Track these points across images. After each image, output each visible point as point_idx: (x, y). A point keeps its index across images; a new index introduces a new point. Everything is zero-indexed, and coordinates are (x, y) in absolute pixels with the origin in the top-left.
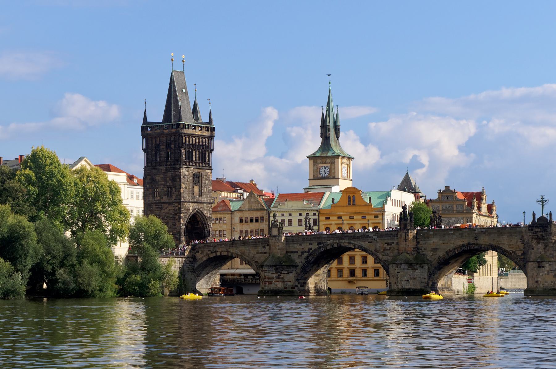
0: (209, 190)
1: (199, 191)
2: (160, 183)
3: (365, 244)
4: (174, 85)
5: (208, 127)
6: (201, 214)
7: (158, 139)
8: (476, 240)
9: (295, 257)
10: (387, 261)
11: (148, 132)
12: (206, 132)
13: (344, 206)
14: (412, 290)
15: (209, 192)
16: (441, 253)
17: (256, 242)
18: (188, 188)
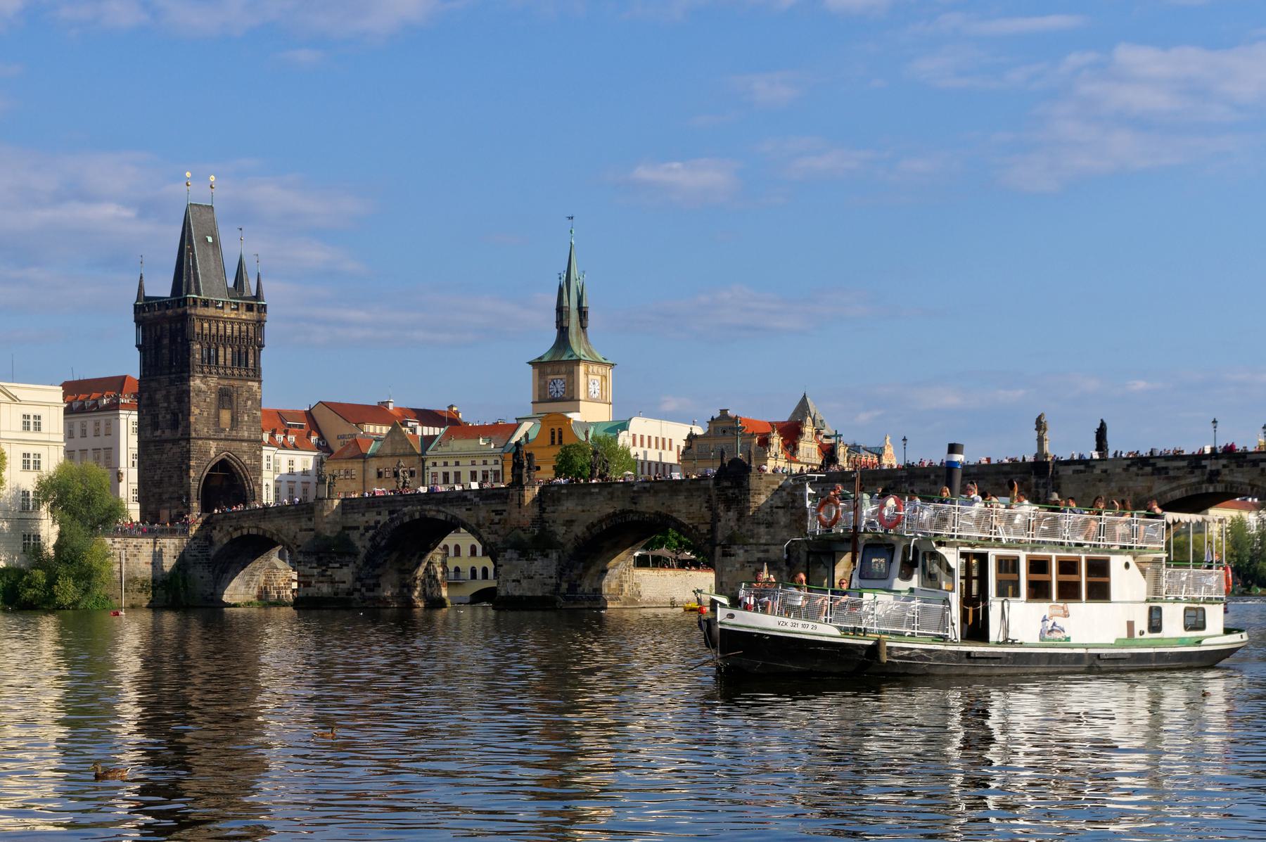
0: (254, 417)
1: (232, 420)
2: (161, 405)
3: (460, 513)
4: (190, 230)
5: (252, 305)
6: (235, 462)
7: (159, 327)
8: (635, 503)
9: (354, 536)
10: (495, 544)
11: (145, 315)
12: (248, 313)
13: (543, 447)
14: (524, 599)
15: (253, 421)
16: (579, 530)
17: (298, 511)
18: (205, 414)
